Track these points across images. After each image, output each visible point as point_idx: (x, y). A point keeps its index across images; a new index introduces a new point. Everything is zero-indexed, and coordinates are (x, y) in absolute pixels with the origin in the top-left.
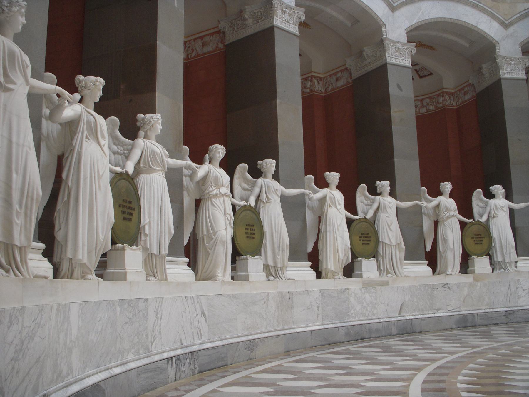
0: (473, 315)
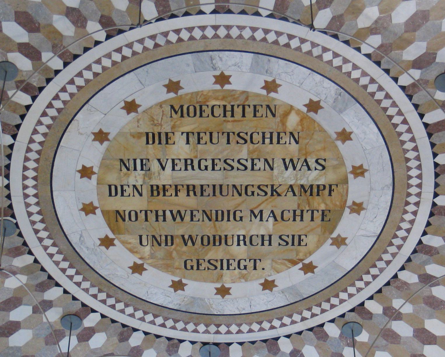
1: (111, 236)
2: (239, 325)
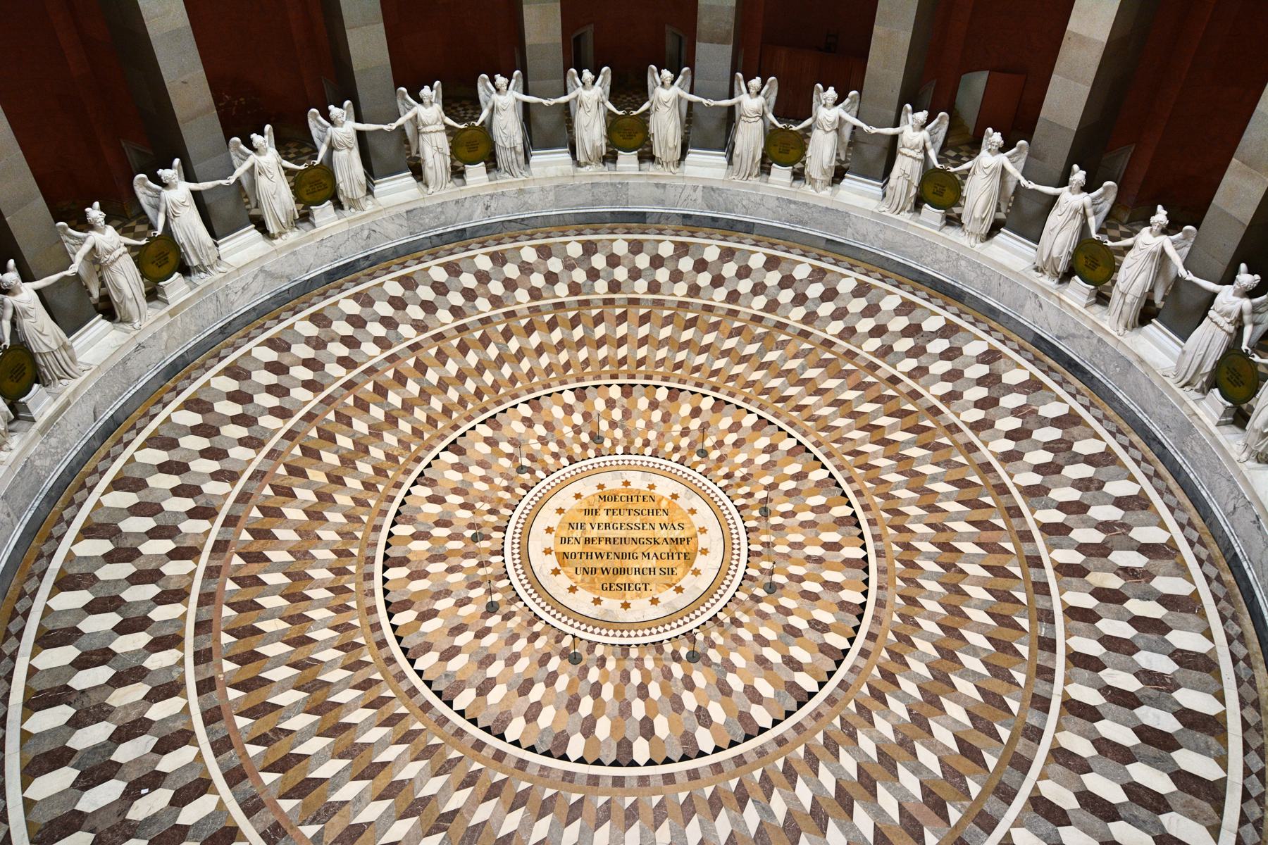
0: (182, 356)
1: (559, 568)
2: (636, 631)
